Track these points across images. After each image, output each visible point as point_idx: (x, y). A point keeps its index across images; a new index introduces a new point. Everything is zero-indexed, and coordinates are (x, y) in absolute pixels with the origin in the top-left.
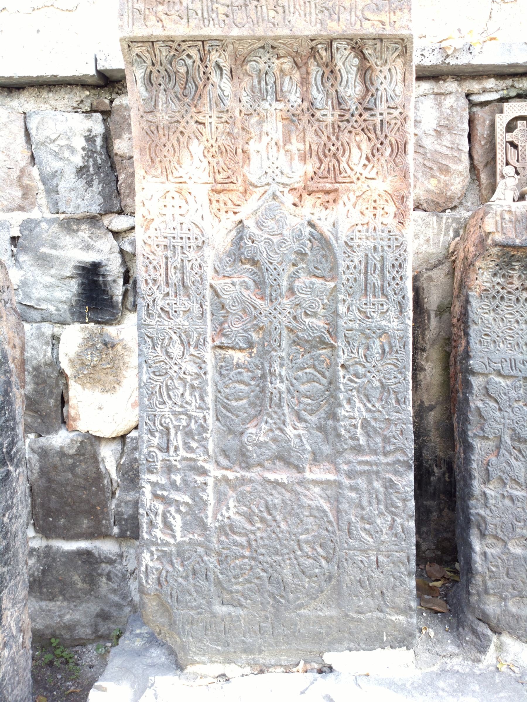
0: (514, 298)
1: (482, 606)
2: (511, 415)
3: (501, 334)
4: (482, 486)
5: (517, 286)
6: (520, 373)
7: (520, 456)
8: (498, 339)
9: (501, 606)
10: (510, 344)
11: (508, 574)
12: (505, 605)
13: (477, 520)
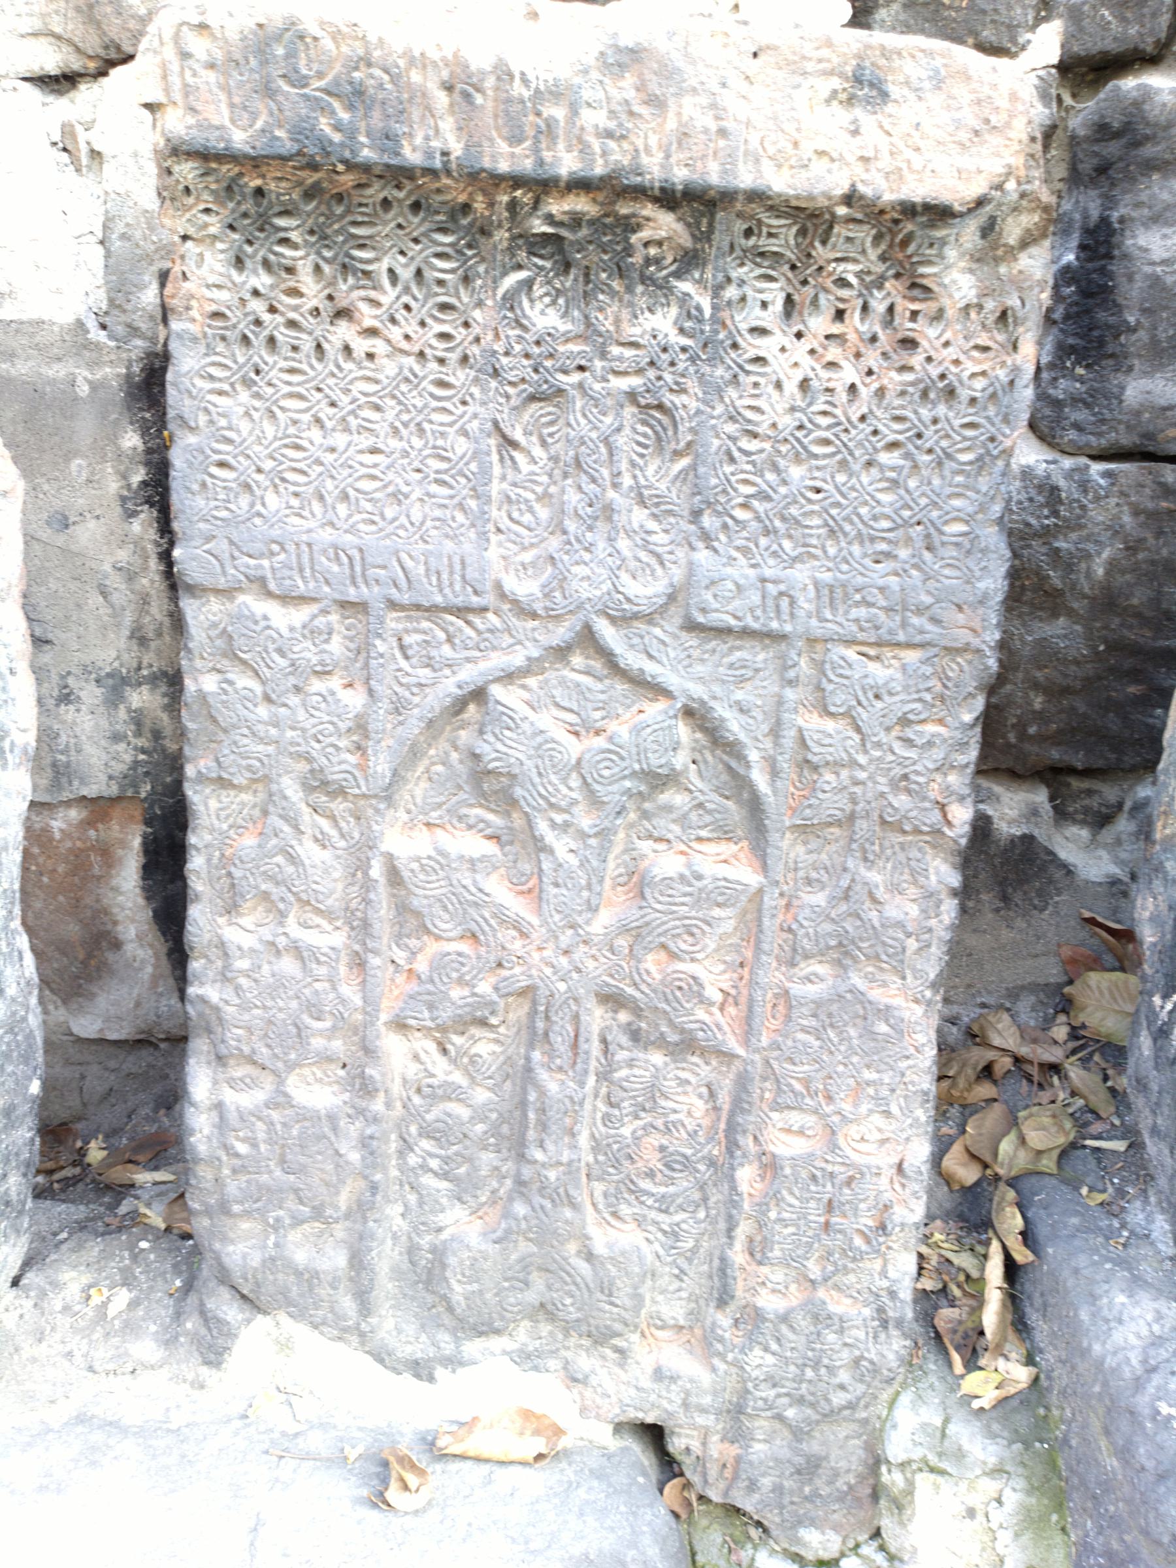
0: (307, 345)
1: (217, 1246)
2: (301, 715)
3: (268, 465)
4: (221, 921)
5: (314, 303)
6: (326, 589)
7: (333, 832)
8: (260, 477)
9: (265, 1247)
10: (296, 495)
11: (282, 1161)
12: (277, 1245)
13: (201, 1015)
